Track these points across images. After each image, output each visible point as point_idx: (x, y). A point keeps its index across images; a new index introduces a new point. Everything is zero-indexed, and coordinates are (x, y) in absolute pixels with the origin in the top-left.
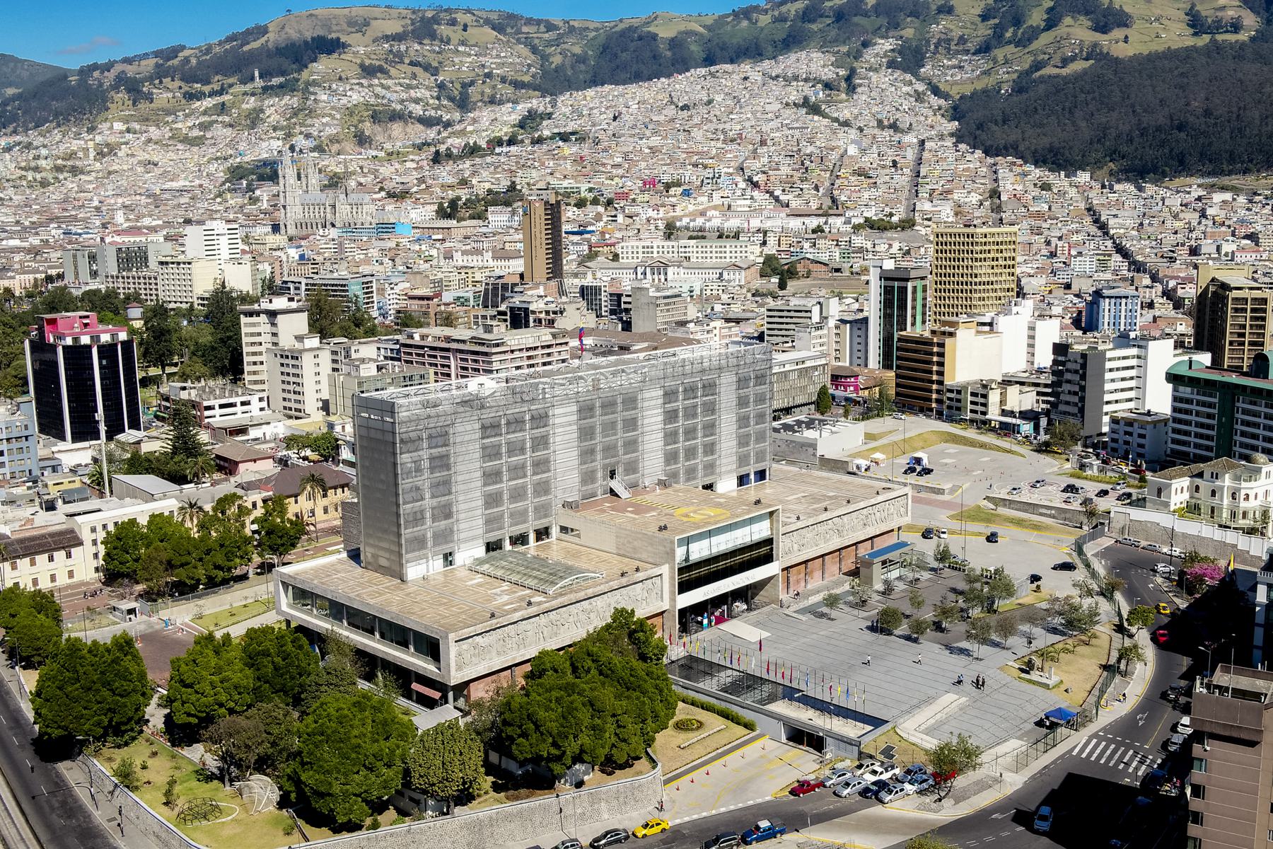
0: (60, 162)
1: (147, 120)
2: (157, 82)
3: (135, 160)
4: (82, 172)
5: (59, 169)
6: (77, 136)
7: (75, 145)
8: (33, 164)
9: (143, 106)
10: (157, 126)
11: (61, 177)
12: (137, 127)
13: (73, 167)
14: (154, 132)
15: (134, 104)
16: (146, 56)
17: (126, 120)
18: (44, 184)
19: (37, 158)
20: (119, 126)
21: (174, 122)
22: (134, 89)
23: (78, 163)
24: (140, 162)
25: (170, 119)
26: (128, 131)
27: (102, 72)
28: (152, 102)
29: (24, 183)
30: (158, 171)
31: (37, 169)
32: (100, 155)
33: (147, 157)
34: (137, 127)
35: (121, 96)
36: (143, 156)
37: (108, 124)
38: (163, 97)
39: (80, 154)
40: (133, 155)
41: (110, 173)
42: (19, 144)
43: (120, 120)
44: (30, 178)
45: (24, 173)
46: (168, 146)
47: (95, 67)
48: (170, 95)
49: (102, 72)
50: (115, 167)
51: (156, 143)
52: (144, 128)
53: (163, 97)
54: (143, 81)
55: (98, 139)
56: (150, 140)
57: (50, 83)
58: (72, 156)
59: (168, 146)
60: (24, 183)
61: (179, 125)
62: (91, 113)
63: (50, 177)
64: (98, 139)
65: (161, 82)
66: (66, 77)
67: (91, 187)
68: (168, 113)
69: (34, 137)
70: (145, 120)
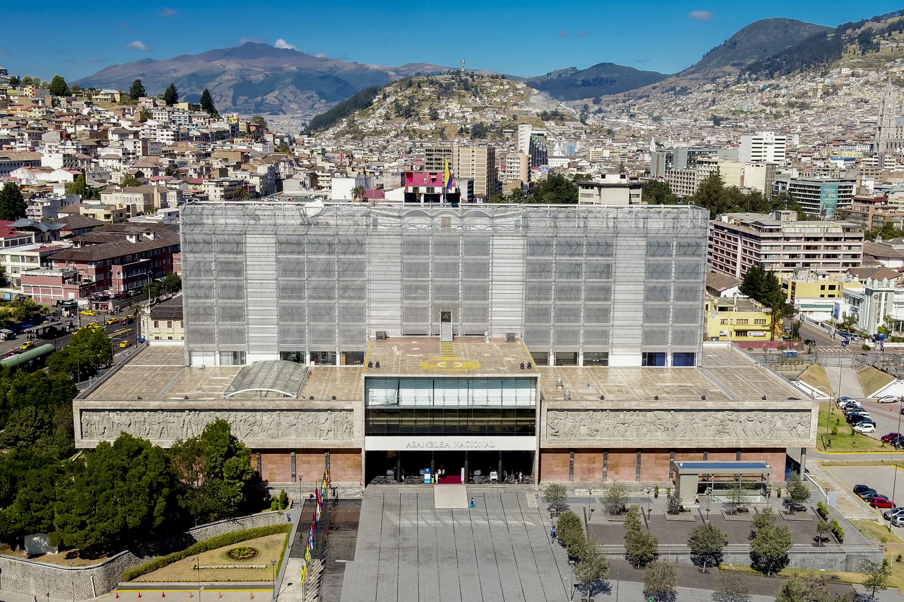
0: (793, 99)
1: (871, 66)
2: (887, 34)
3: (850, 99)
4: (808, 108)
5: (791, 105)
6: (813, 79)
7: (808, 86)
8: (772, 101)
9: (871, 54)
10: (877, 71)
11: (791, 111)
12: (861, 71)
13: (802, 103)
14: (873, 75)
15: (863, 53)
16: (893, 15)
17: (852, 67)
18: (777, 116)
19: (777, 96)
20: (846, 71)
21: (891, 67)
22: (866, 42)
23: (807, 101)
24: (854, 100)
25: (888, 65)
26: (853, 75)
27: (854, 30)
28: (878, 51)
29: (763, 115)
30: (866, 107)
31: (775, 105)
32: (826, 93)
33: (861, 95)
34: (861, 71)
35: (856, 46)
36: (858, 95)
37: (838, 70)
38: (887, 46)
39: (810, 94)
40: (850, 94)
41: (828, 108)
42: (770, 86)
43: (848, 66)
44: (768, 112)
45: (764, 107)
46: (881, 86)
47: (849, 26)
48: (894, 45)
49: (854, 30)
50: (833, 104)
51: (872, 84)
52: (866, 72)
53: (887, 46)
54: (874, 36)
55: (828, 81)
56: (867, 82)
57: (812, 39)
58: (804, 94)
59: (881, 86)
60: (763, 115)
61: (894, 70)
62: (827, 62)
63: (782, 111)
64: (828, 81)
65: (890, 35)
66: (825, 34)
67: (809, 119)
68: (889, 59)
69: (783, 81)
70: (869, 66)
